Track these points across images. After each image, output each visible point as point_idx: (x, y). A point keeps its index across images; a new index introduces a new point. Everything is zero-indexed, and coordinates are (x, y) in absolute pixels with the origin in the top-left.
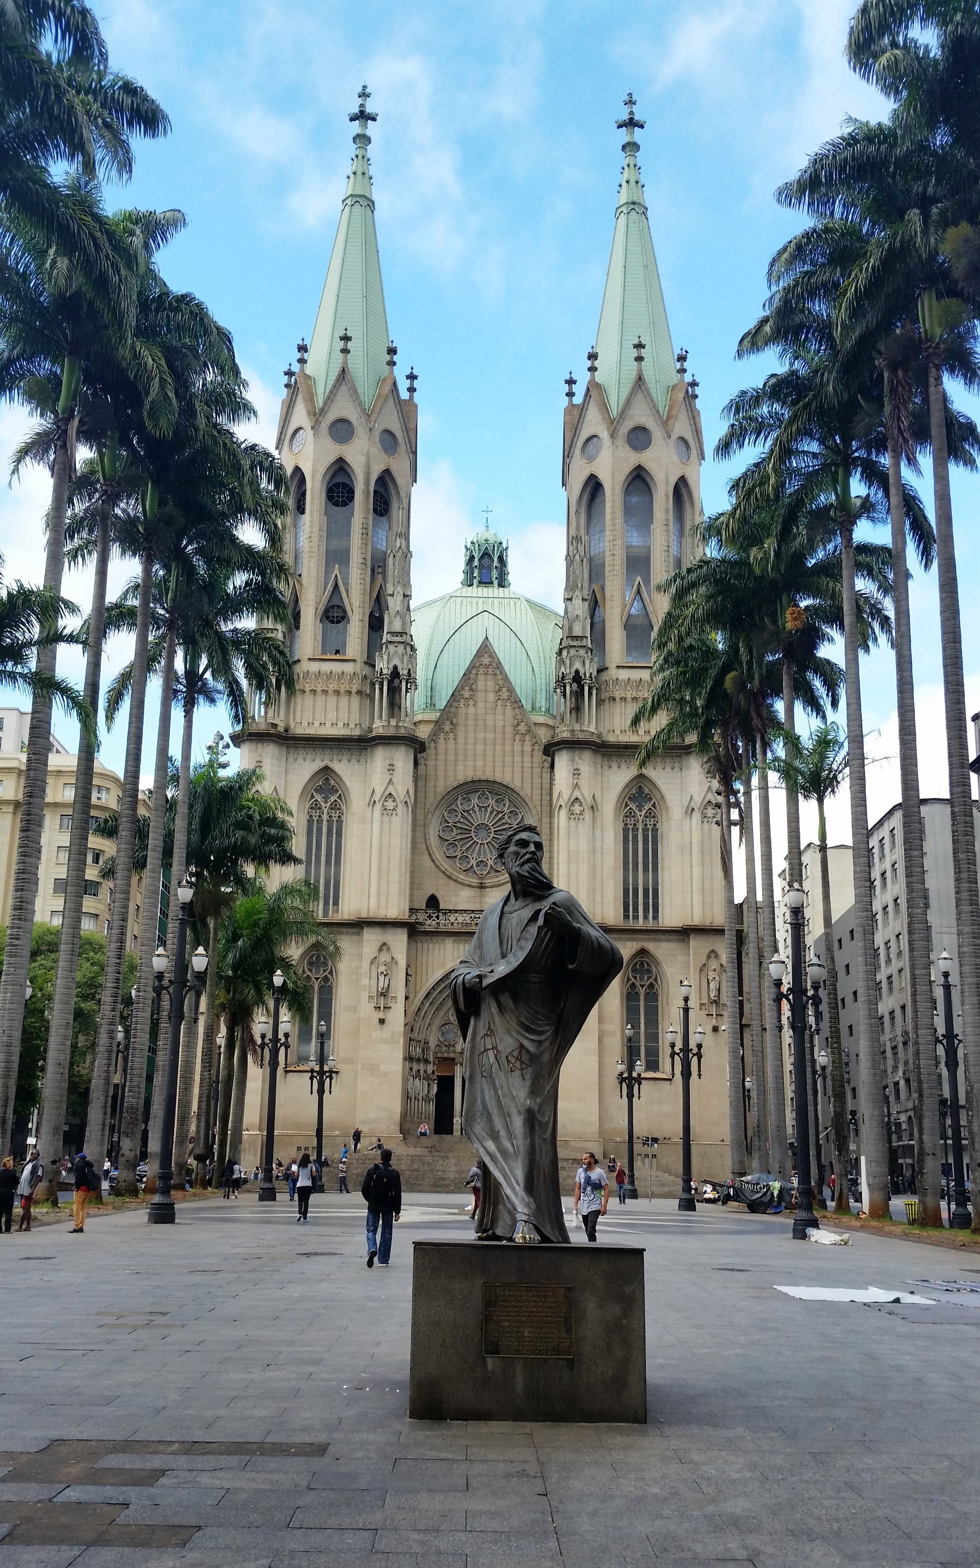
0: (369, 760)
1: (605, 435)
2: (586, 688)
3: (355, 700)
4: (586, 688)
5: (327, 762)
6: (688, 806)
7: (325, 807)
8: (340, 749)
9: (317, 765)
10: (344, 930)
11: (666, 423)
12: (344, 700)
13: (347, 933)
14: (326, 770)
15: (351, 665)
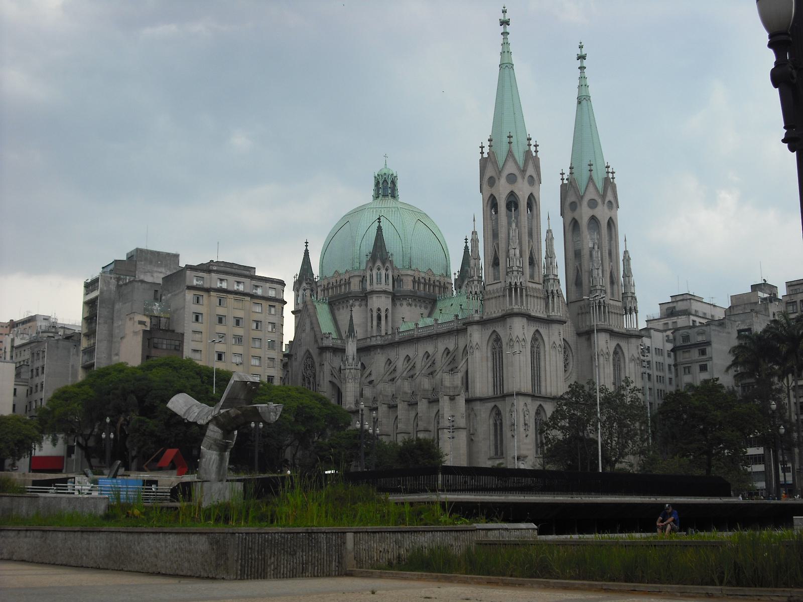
0: (550, 329)
1: (599, 201)
2: (602, 307)
3: (542, 301)
4: (602, 307)
5: (537, 328)
6: (631, 358)
7: (536, 346)
8: (545, 323)
9: (535, 328)
10: (548, 400)
11: (603, 196)
12: (539, 300)
13: (549, 402)
14: (537, 331)
15: (540, 285)
